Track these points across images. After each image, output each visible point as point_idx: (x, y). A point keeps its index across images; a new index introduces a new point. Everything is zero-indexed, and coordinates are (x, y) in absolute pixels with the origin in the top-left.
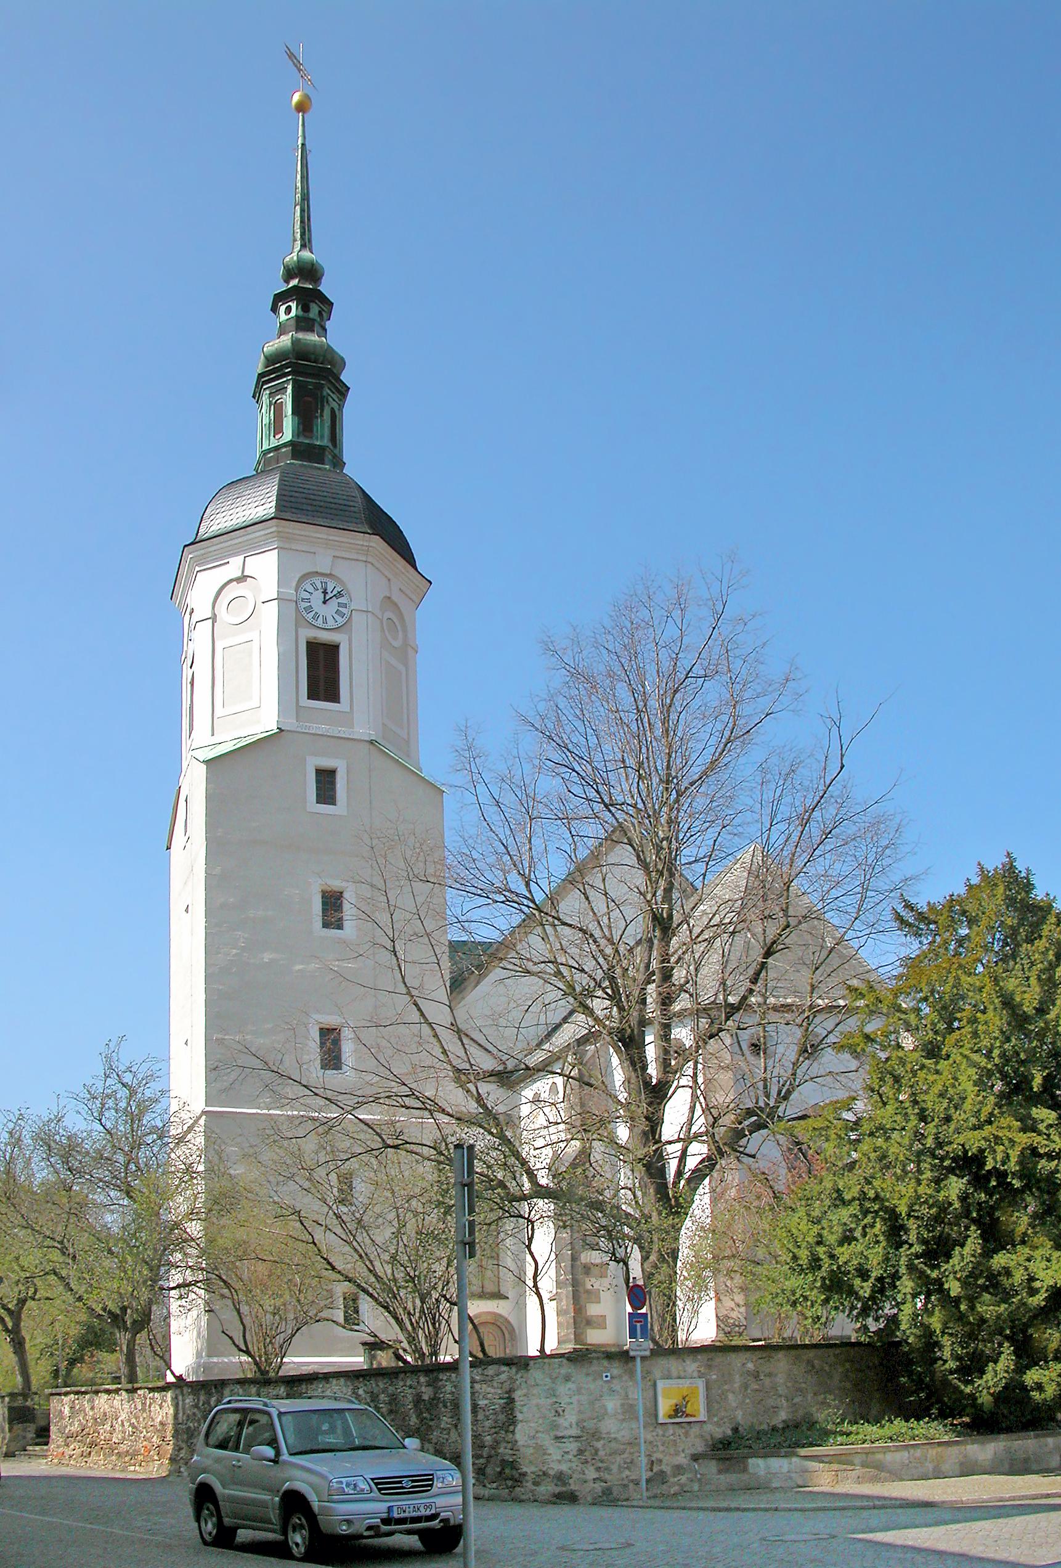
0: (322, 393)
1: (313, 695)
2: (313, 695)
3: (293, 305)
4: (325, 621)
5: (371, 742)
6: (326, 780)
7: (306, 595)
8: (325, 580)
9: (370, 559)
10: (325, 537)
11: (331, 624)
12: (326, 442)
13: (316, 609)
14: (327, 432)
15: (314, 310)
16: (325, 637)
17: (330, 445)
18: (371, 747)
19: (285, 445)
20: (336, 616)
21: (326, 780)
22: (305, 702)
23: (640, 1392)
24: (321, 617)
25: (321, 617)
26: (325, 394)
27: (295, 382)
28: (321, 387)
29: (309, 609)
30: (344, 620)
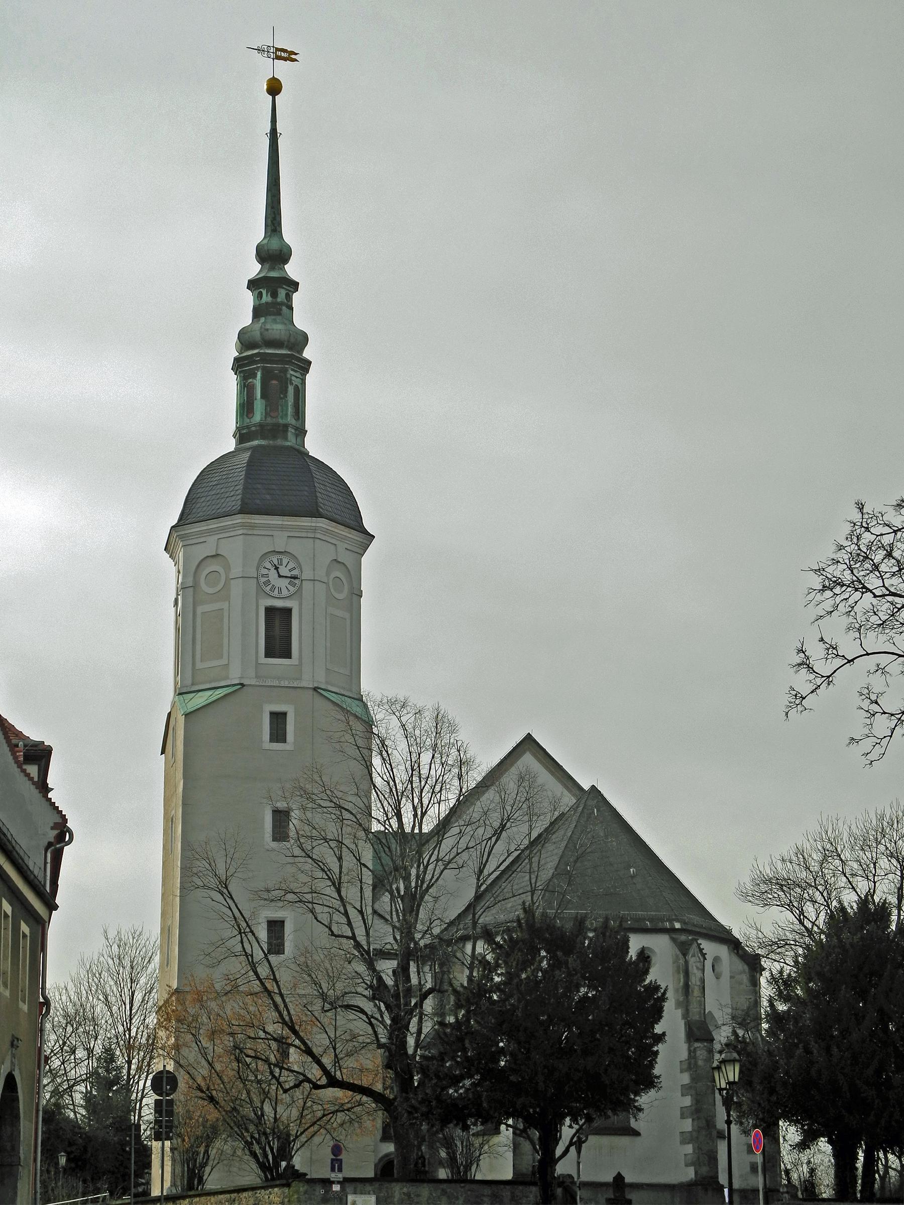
0: (286, 375)
1: (270, 653)
2: (270, 653)
3: (264, 292)
4: (280, 590)
5: (315, 689)
6: (279, 718)
7: (265, 572)
8: (280, 557)
9: (318, 536)
10: (280, 523)
11: (285, 593)
12: (290, 419)
13: (273, 583)
14: (290, 410)
15: (282, 294)
16: (279, 604)
17: (293, 422)
18: (315, 693)
19: (255, 425)
20: (289, 587)
21: (279, 718)
22: (263, 660)
23: (723, 1179)
24: (277, 589)
25: (277, 589)
26: (289, 376)
27: (264, 369)
28: (286, 370)
29: (267, 583)
30: (296, 589)
